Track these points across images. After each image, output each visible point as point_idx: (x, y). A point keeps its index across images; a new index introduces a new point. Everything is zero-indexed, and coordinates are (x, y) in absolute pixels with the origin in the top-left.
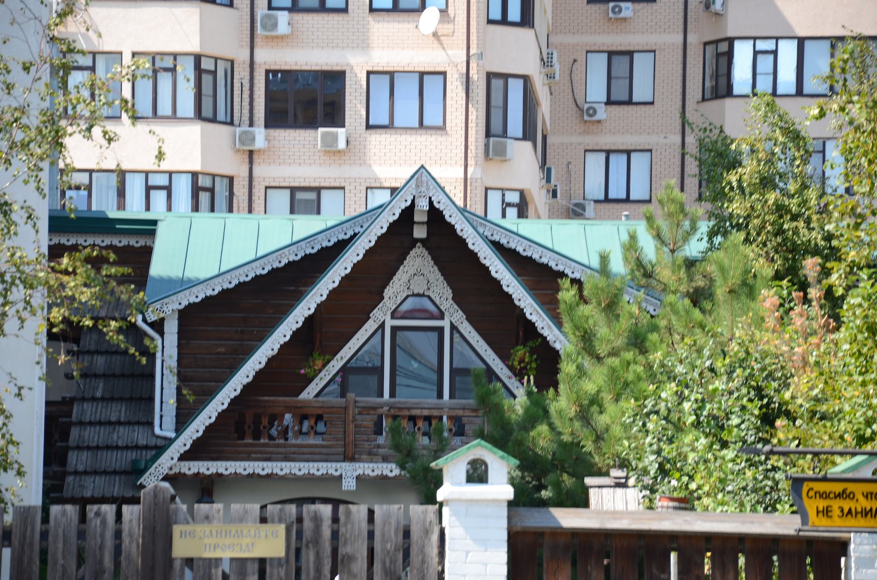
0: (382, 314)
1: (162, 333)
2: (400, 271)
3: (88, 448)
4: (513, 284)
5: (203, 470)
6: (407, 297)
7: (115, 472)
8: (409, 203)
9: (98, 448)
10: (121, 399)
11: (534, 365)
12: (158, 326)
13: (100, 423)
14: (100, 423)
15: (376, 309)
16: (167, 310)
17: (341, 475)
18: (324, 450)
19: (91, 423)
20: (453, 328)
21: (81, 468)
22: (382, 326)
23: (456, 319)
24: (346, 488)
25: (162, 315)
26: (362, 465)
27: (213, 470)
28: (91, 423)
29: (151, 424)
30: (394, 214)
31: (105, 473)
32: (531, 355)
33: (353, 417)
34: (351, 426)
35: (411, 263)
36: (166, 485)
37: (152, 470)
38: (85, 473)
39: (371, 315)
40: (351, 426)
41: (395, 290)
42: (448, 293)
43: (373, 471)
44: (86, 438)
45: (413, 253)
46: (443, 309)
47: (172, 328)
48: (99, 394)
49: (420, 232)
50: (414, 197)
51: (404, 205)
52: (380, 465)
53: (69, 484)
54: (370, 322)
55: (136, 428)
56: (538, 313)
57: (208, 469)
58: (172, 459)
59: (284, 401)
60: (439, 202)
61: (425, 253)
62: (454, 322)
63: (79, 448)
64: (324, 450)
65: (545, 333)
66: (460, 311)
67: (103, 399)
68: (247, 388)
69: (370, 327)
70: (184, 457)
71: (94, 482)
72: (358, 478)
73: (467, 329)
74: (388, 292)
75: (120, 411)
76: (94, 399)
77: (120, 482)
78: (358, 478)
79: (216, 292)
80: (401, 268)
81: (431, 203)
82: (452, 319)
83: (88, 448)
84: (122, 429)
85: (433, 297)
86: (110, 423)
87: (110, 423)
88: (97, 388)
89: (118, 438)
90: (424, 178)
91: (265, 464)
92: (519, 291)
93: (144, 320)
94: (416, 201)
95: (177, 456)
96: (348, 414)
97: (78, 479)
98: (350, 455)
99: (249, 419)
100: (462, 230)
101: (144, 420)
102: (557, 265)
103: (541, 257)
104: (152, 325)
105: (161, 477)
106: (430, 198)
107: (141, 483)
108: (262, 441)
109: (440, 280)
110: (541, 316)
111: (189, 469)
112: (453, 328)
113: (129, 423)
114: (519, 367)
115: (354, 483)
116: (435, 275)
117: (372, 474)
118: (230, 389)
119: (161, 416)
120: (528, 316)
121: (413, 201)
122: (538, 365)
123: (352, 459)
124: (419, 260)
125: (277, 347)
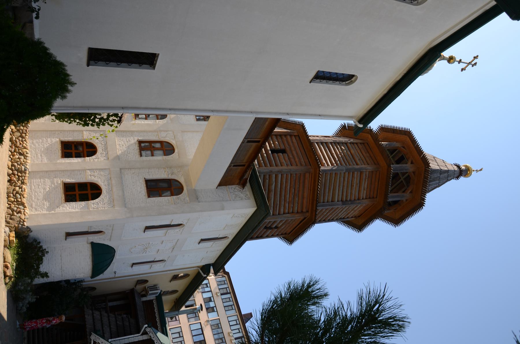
1: (142, 334)
3: (101, 318)
7: (94, 326)
9: (102, 321)
12: (145, 333)
13: (109, 322)
14: (109, 322)
19: (109, 319)
21: (95, 315)
25: (148, 333)
28: (109, 319)
29: (111, 338)
31: (94, 323)
37: (97, 336)
38: (93, 316)
47: (145, 337)
48: (118, 322)
63: (101, 315)
67: (117, 324)
71: (90, 319)
76: (116, 321)
83: (101, 318)
84: (109, 329)
86: (110, 325)
87: (110, 325)
93: (146, 327)
104: (145, 330)
105: (95, 340)
107: (92, 334)
119: (115, 341)
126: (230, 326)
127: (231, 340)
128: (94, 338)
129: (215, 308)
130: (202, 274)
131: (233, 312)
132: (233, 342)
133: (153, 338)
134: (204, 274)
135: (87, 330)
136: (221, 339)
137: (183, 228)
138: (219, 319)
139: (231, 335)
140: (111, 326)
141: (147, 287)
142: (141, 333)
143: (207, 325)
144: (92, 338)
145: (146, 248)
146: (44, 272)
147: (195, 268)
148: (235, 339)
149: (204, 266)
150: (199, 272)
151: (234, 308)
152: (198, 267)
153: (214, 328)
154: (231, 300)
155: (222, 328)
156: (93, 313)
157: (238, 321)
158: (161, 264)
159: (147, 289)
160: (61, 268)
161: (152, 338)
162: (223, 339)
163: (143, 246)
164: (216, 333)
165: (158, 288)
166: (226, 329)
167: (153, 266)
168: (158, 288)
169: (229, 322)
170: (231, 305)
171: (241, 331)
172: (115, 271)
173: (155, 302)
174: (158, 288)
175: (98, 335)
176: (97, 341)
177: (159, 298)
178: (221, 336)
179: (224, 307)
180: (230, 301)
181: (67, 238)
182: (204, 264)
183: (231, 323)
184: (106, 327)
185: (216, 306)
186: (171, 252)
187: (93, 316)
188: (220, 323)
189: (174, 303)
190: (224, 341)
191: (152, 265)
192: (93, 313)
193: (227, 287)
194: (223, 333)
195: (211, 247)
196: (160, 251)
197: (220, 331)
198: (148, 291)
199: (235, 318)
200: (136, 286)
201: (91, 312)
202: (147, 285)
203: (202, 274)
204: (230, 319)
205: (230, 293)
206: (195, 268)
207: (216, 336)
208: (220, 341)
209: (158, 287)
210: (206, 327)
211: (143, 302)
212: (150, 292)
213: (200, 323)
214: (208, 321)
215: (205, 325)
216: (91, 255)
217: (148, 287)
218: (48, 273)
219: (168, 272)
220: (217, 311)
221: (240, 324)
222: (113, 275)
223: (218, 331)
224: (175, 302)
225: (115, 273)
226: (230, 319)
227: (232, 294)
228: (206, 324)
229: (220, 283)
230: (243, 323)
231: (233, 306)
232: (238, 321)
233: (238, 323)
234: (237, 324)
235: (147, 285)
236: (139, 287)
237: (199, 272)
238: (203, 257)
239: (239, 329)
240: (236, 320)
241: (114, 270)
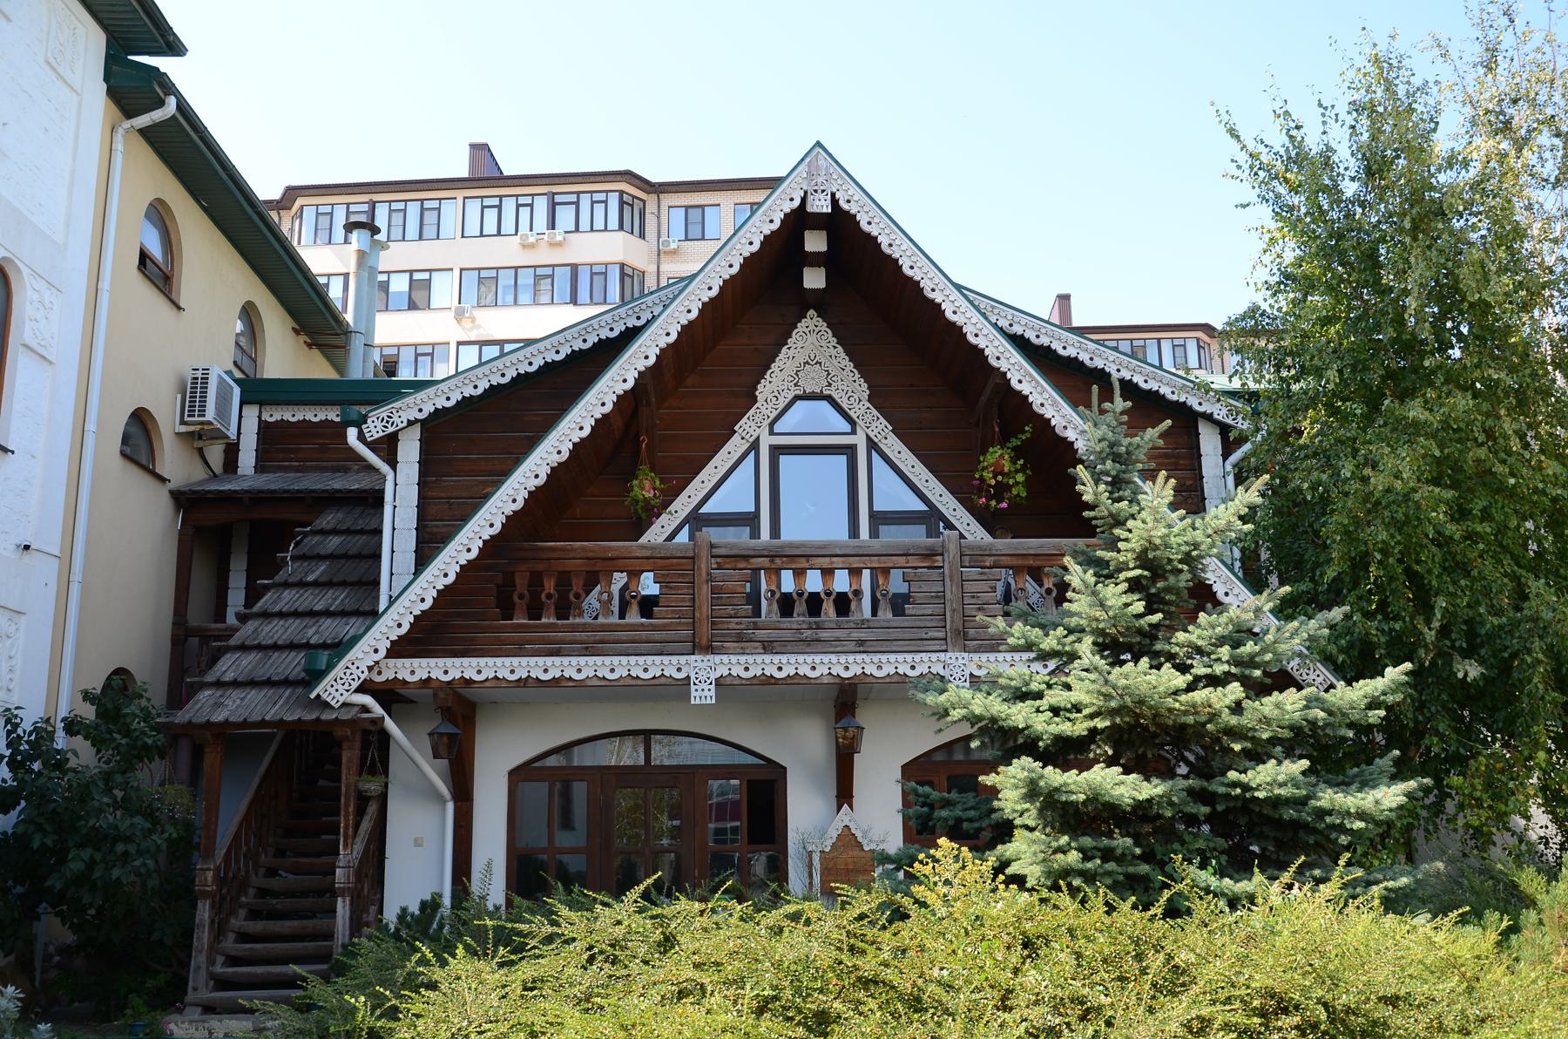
0: (754, 427)
1: (393, 462)
2: (781, 356)
3: (260, 647)
4: (985, 331)
5: (437, 674)
6: (797, 398)
7: (286, 683)
8: (797, 203)
9: (275, 647)
10: (343, 584)
11: (1020, 477)
12: (388, 447)
13: (296, 614)
14: (296, 614)
15: (745, 419)
16: (399, 421)
17: (688, 678)
18: (657, 635)
20: (872, 445)
21: (229, 676)
22: (755, 446)
23: (876, 431)
24: (698, 702)
25: (391, 430)
26: (725, 658)
27: (455, 674)
28: (281, 615)
30: (771, 221)
31: (269, 683)
32: (1013, 461)
33: (709, 574)
34: (705, 591)
35: (800, 344)
36: (367, 700)
37: (338, 671)
38: (235, 684)
39: (736, 428)
40: (705, 591)
41: (773, 387)
42: (863, 389)
43: (747, 669)
44: (263, 634)
45: (801, 326)
46: (854, 416)
47: (410, 450)
48: (310, 578)
49: (814, 279)
50: (806, 192)
51: (788, 207)
52: (759, 658)
53: (199, 701)
54: (736, 439)
55: (353, 620)
56: (1033, 379)
57: (446, 672)
58: (376, 651)
59: (583, 549)
60: (849, 201)
61: (823, 325)
62: (872, 435)
64: (657, 635)
65: (1048, 412)
66: (882, 419)
68: (512, 521)
69: (735, 446)
70: (399, 649)
71: (242, 699)
72: (719, 682)
73: (894, 446)
74: (764, 390)
75: (335, 599)
77: (289, 697)
78: (719, 682)
79: (480, 391)
80: (784, 349)
81: (834, 202)
82: (869, 431)
83: (260, 647)
84: (329, 621)
85: (836, 397)
86: (312, 614)
87: (312, 614)
88: (313, 572)
89: (316, 633)
90: (821, 162)
91: (549, 660)
92: (996, 343)
94: (810, 198)
95: (384, 646)
96: (699, 568)
97: (219, 693)
98: (704, 642)
99: (521, 581)
100: (890, 245)
101: (367, 608)
102: (1038, 337)
103: (1011, 325)
104: (373, 446)
105: (355, 685)
106: (833, 195)
107: (318, 696)
108: (544, 620)
109: (847, 369)
110: (1037, 382)
111: (413, 672)
112: (872, 445)
113: (343, 614)
114: (993, 482)
115: (713, 693)
116: (839, 361)
117: (744, 675)
118: (483, 523)
120: (1014, 384)
121: (804, 200)
122: (1028, 478)
123: (709, 649)
124: (812, 338)
125: (566, 448)
126: (499, 234)
127: (553, 245)
128: (340, 687)
129: (417, 276)
130: (157, 115)
131: (451, 211)
132: (559, 238)
133: (420, 410)
134: (161, 103)
135: (291, 717)
136: (538, 278)
138: (461, 270)
139: (532, 240)
140: (317, 608)
141: (183, 429)
142: (384, 468)
143: (473, 320)
144: (342, 700)
148: (553, 228)
149: (113, 93)
150: (145, 133)
151: (435, 204)
153: (491, 297)
154: (401, 206)
155: (497, 269)
156: (219, 684)
157: (487, 202)
158: (29, 292)
159: (191, 428)
161: (421, 416)
162: (540, 271)
164: (510, 299)
165: (200, 376)
166: (506, 252)
167: (28, 338)
168: (201, 372)
169: (482, 235)
170: (423, 210)
171: (528, 200)
173: (274, 415)
174: (199, 374)
175: (330, 666)
176: (363, 677)
177: (257, 391)
178: (526, 278)
179: (421, 238)
180: (405, 211)
183: (491, 227)
184: (311, 632)
185: (411, 272)
187: (235, 684)
188: (479, 269)
189: (316, 352)
190: (548, 271)
191: (25, 345)
192: (219, 684)
193: (348, 208)
194: (516, 268)
197: (506, 279)
198: (202, 423)
199: (474, 208)
200: (162, 480)
201: (207, 693)
202: (167, 421)
203: (157, 115)
204: (473, 227)
205: (373, 205)
206: (119, 145)
207: (525, 297)
208: (545, 284)
209: (189, 375)
210: (479, 326)
211: (260, 467)
212: (210, 414)
213: (459, 343)
214: (459, 315)
215: (471, 329)
217: (183, 422)
219: (105, 284)
220: (430, 271)
221: (501, 197)
222: (45, 571)
223: (505, 287)
224: (309, 346)
225: (27, 547)
226: (473, 227)
227: (376, 197)
228: (467, 324)
229: (324, 235)
230: (501, 182)
231: (427, 204)
232: (487, 202)
233: (496, 202)
234: (499, 207)
235: (167, 421)
236: (177, 465)
237: (145, 133)
239: (518, 206)
240: (483, 207)
241: (10, 552)
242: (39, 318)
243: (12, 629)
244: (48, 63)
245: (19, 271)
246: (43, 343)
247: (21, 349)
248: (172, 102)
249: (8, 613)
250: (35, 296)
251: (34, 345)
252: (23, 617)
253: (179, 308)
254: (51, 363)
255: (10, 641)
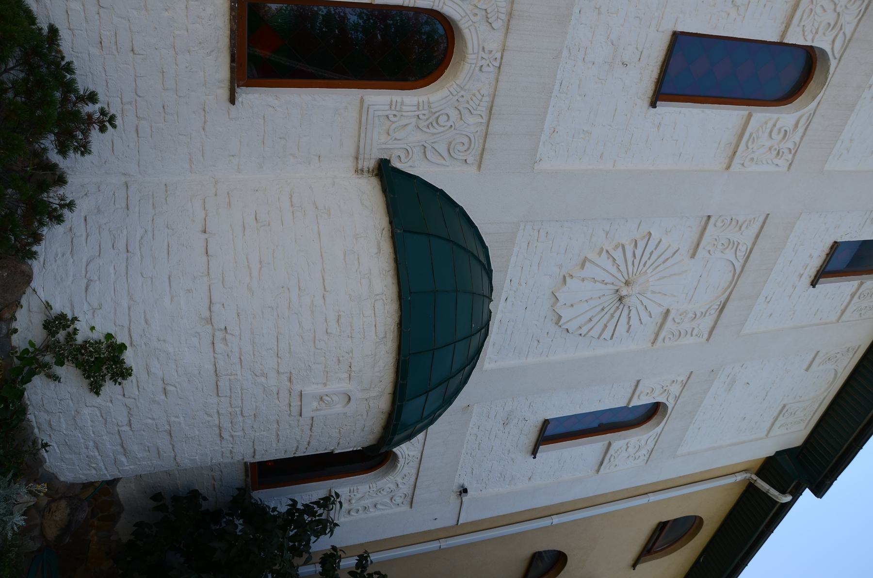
130: (773, 493)
134: (783, 492)
137: (814, 104)
145: (627, 283)
146: (96, 336)
147: (731, 480)
152: (746, 471)
158: (645, 437)
160: (206, 314)
163: (618, 254)
172: (461, 482)
181: (238, 90)
182: (771, 453)
186: (706, 336)
191: (610, 444)
195: (838, 321)
196: (669, 324)
203: (773, 493)
216: (387, 234)
218: (123, 347)
219: (653, 498)
238: (784, 402)
242: (629, 450)
243: (398, 500)
244: (784, 406)
245: (658, 424)
246: (612, 459)
247: (606, 443)
248: (788, 498)
249: (410, 493)
250: (643, 442)
251: (611, 451)
252: (409, 506)
253: (634, 566)
254: (598, 471)
255: (387, 500)
